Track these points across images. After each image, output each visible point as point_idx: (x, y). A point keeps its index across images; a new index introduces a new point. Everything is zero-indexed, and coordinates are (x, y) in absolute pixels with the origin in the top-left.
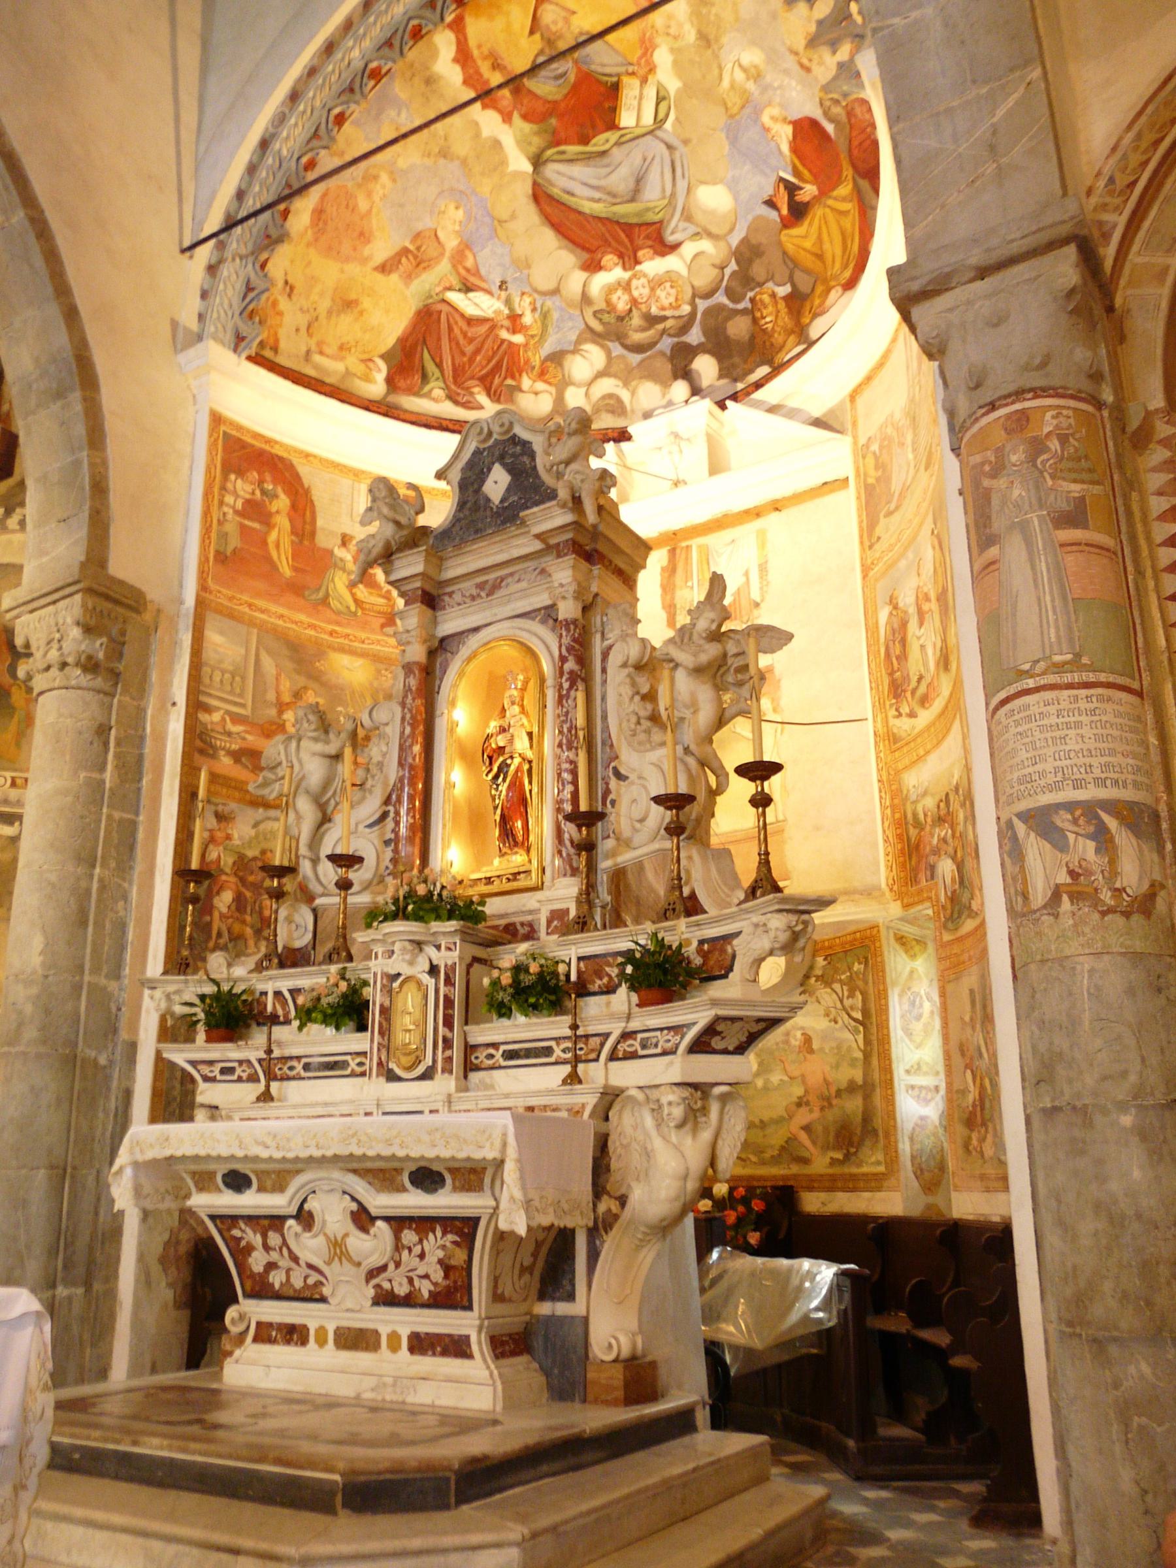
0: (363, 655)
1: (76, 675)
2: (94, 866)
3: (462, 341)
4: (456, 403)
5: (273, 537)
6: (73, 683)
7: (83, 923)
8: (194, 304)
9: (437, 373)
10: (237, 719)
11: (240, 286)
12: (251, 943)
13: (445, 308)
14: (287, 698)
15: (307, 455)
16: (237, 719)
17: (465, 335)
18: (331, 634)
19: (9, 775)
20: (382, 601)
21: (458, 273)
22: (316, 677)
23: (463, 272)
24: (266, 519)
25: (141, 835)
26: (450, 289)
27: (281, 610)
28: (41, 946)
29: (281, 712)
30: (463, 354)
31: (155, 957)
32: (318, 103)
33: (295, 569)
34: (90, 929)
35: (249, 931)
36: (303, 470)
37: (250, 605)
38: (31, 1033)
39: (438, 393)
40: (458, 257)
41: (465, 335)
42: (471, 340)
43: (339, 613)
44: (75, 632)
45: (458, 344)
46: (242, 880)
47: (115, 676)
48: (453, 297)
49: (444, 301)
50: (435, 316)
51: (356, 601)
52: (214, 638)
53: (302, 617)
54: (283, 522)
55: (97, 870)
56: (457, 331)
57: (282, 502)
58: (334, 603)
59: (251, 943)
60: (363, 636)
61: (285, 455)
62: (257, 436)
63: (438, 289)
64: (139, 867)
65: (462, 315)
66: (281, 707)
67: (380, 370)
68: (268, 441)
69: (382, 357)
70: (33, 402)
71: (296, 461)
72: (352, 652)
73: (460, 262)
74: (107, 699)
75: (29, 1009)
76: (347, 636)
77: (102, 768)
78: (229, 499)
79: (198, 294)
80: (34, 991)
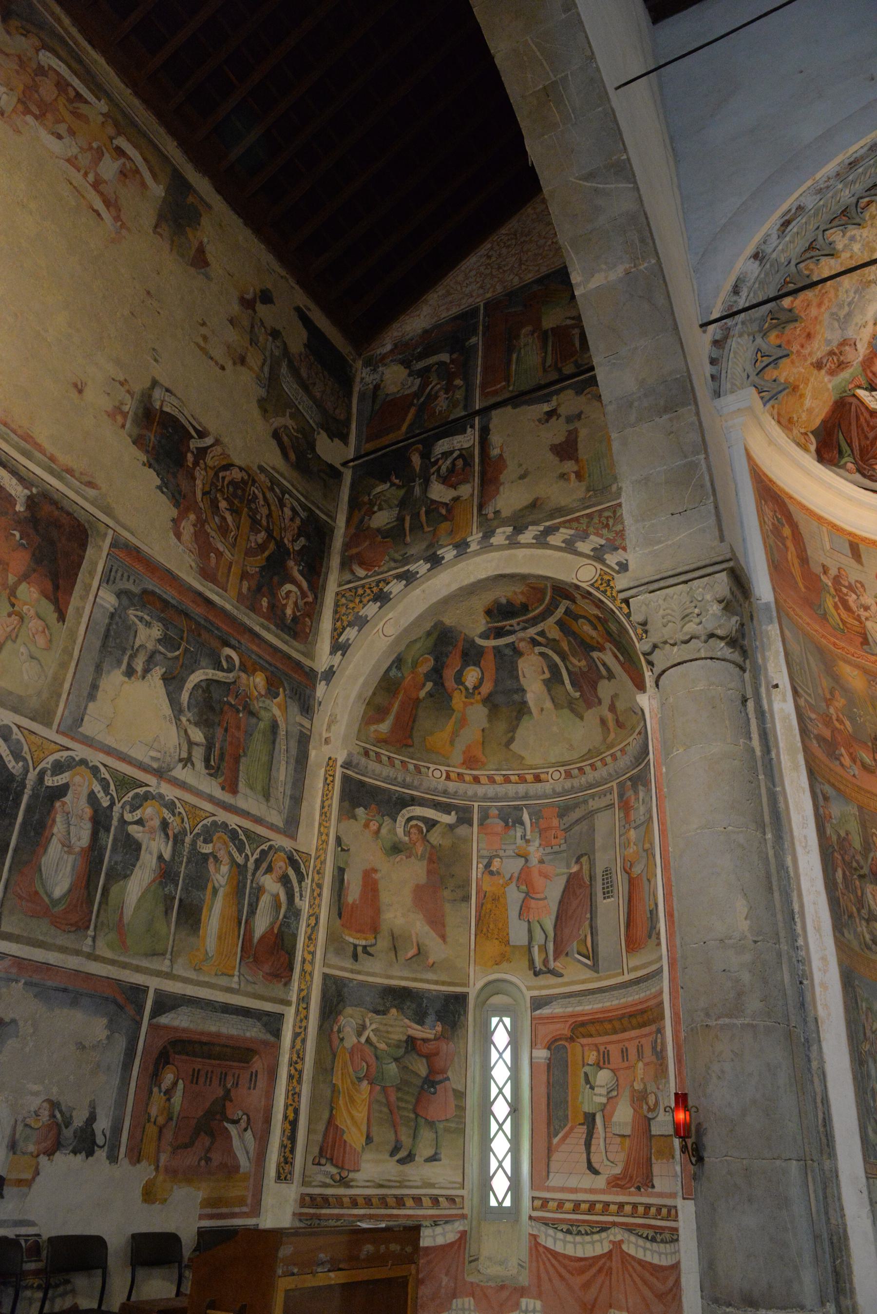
0: (857, 666)
1: (720, 648)
2: (764, 833)
3: (866, 428)
4: (864, 475)
5: (789, 557)
6: (719, 654)
7: (770, 889)
8: (708, 369)
9: (849, 452)
10: (812, 708)
11: (750, 354)
12: (857, 920)
13: (853, 400)
14: (828, 696)
15: (791, 498)
16: (812, 708)
17: (868, 423)
18: (834, 644)
19: (443, 768)
20: (856, 623)
21: (867, 375)
22: (836, 678)
23: (870, 375)
24: (783, 540)
25: (782, 805)
26: (859, 387)
27: (808, 620)
28: (746, 910)
29: (828, 706)
30: (867, 438)
31: (818, 929)
32: (812, 227)
33: (806, 587)
34: (776, 895)
35: (855, 910)
36: (792, 508)
37: (794, 610)
38: (754, 1004)
39: (850, 466)
40: (867, 363)
41: (868, 423)
42: (872, 428)
43: (834, 629)
44: (716, 608)
45: (863, 429)
46: (843, 859)
47: (744, 653)
48: (862, 393)
49: (854, 395)
50: (848, 407)
51: (841, 620)
52: (787, 633)
53: (817, 628)
54: (790, 544)
55: (769, 836)
56: (862, 420)
57: (787, 531)
58: (831, 620)
59: (857, 920)
60: (852, 650)
61: (779, 492)
62: (765, 474)
63: (851, 386)
64: (787, 837)
65: (867, 408)
66: (828, 702)
67: (812, 444)
68: (771, 481)
69: (812, 432)
70: (633, 418)
71: (787, 500)
72: (849, 663)
73: (869, 367)
74: (741, 673)
75: (746, 977)
76: (843, 648)
77: (750, 739)
78: (766, 519)
79: (707, 361)
80: (747, 957)
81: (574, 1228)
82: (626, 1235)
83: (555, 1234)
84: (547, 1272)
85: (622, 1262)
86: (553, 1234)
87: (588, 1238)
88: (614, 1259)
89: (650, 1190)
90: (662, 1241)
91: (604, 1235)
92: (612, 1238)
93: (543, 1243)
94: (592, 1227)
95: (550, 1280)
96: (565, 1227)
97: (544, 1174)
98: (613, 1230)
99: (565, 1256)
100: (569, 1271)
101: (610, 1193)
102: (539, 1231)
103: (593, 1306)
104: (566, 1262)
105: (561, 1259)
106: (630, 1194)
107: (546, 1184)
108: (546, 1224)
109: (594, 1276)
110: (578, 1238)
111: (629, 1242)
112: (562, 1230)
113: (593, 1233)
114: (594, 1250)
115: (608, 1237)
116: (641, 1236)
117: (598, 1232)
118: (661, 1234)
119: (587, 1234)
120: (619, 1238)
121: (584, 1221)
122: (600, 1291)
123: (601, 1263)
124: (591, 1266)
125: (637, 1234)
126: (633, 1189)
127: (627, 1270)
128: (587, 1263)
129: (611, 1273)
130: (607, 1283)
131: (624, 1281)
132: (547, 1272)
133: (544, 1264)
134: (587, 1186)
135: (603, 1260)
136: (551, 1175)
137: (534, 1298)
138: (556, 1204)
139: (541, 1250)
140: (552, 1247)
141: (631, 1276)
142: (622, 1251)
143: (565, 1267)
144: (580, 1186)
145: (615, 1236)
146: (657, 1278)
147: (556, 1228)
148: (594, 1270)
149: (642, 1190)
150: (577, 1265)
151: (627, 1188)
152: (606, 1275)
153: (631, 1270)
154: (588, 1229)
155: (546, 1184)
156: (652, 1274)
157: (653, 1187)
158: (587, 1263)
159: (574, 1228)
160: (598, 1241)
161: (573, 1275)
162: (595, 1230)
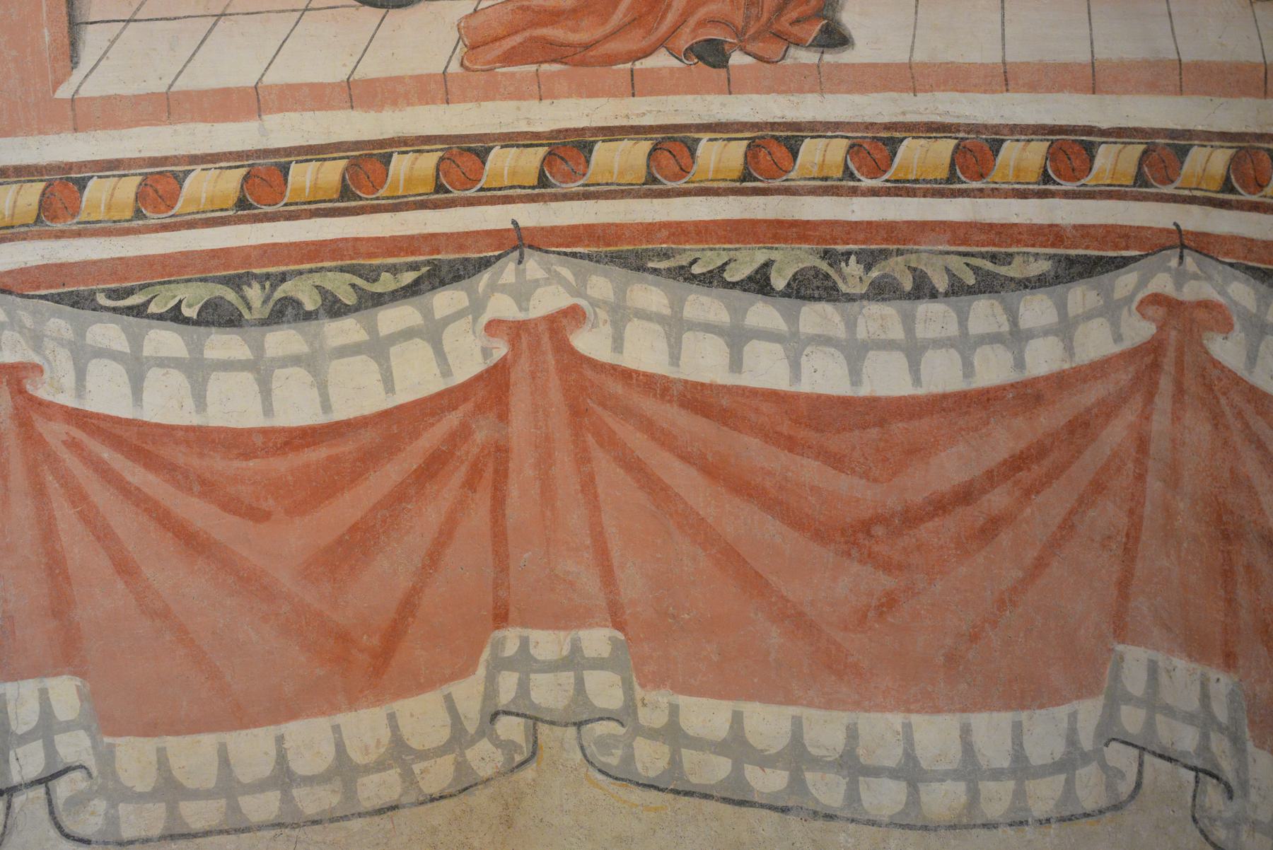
81: (254, 293)
82: (601, 285)
83: (136, 341)
84: (103, 534)
85: (577, 412)
86: (68, 334)
87: (345, 330)
88: (520, 400)
89: (806, 57)
90: (882, 291)
91: (446, 300)
92: (503, 307)
93: (67, 399)
94: (372, 275)
95: (125, 568)
96: (192, 297)
97: (48, 35)
98: (508, 271)
99: (202, 438)
100: (231, 505)
101: (489, 93)
102: (37, 341)
103: (393, 636)
104: (219, 464)
105: (179, 456)
106: (634, 87)
107: (64, 92)
108: (78, 301)
109: (399, 497)
110: (283, 340)
111: (620, 315)
112: (175, 315)
113: (378, 300)
114: (388, 383)
115: (477, 307)
116: (713, 279)
117: (412, 291)
118: (869, 260)
119: (334, 308)
120: (548, 301)
121: (314, 251)
122: (433, 558)
123: (432, 437)
124: (369, 459)
125: (683, 274)
126: (661, 60)
127: (609, 441)
128: (347, 448)
129: (501, 475)
130: (478, 515)
131: (588, 484)
132: (103, 534)
133: (77, 496)
134: (332, 71)
135: (452, 420)
136: (93, 40)
137: (37, 671)
138: (128, 187)
139: (54, 432)
140: (123, 410)
141: (634, 466)
142: (574, 362)
143: (208, 488)
144: (275, 77)
145: (522, 295)
146: (836, 461)
147: (138, 311)
148: (391, 474)
149: (737, 59)
150: (282, 465)
151: (610, 60)
152: (470, 484)
153: (637, 441)
154: (341, 285)
155: (64, 92)
156: (791, 445)
157: (835, 38)
158: (347, 448)
159: (254, 293)
160: (408, 334)
161: (257, 515)
162: (386, 283)
